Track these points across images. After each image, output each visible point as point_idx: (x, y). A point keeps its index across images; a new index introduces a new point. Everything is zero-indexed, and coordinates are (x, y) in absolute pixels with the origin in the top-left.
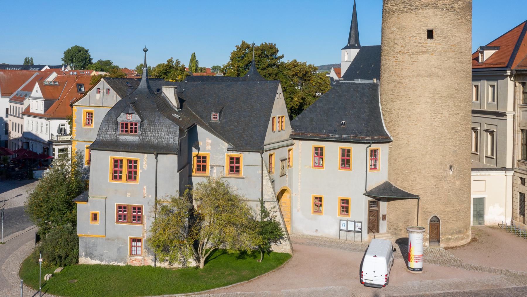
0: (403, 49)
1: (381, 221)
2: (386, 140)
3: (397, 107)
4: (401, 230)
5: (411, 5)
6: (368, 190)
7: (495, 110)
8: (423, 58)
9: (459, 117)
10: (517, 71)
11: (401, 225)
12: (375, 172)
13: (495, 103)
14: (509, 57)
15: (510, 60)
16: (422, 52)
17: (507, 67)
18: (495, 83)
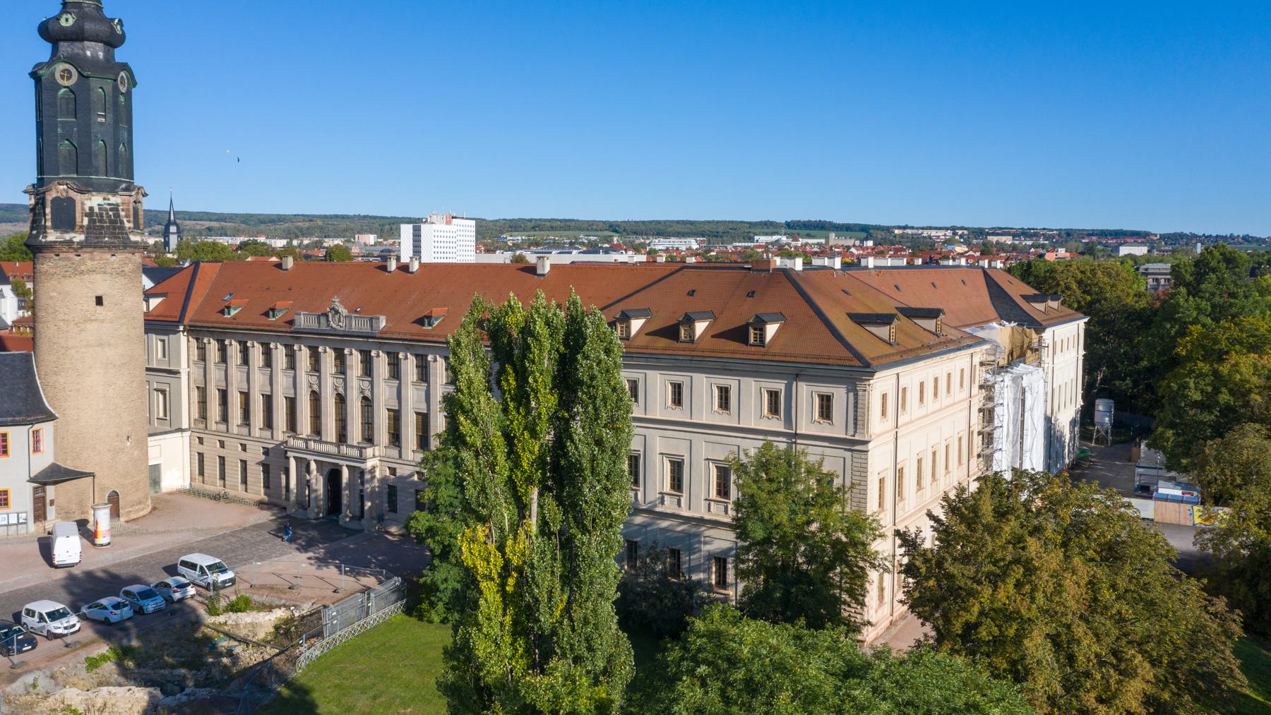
0: (66, 317)
1: (48, 508)
2: (50, 417)
3: (62, 381)
4: (74, 513)
5: (75, 269)
6: (32, 476)
7: (167, 367)
8: (91, 327)
9: (135, 385)
10: (190, 326)
11: (74, 507)
12: (38, 454)
13: (167, 359)
14: (180, 309)
15: (181, 313)
16: (91, 320)
17: (179, 322)
18: (165, 338)
